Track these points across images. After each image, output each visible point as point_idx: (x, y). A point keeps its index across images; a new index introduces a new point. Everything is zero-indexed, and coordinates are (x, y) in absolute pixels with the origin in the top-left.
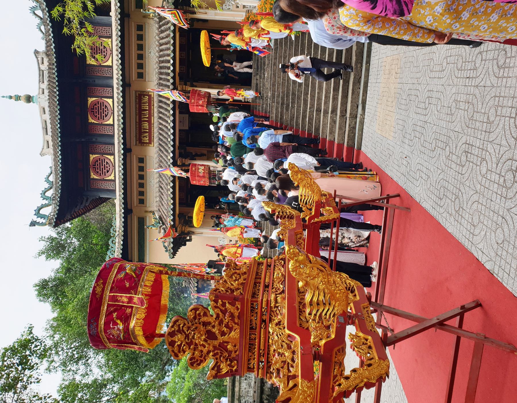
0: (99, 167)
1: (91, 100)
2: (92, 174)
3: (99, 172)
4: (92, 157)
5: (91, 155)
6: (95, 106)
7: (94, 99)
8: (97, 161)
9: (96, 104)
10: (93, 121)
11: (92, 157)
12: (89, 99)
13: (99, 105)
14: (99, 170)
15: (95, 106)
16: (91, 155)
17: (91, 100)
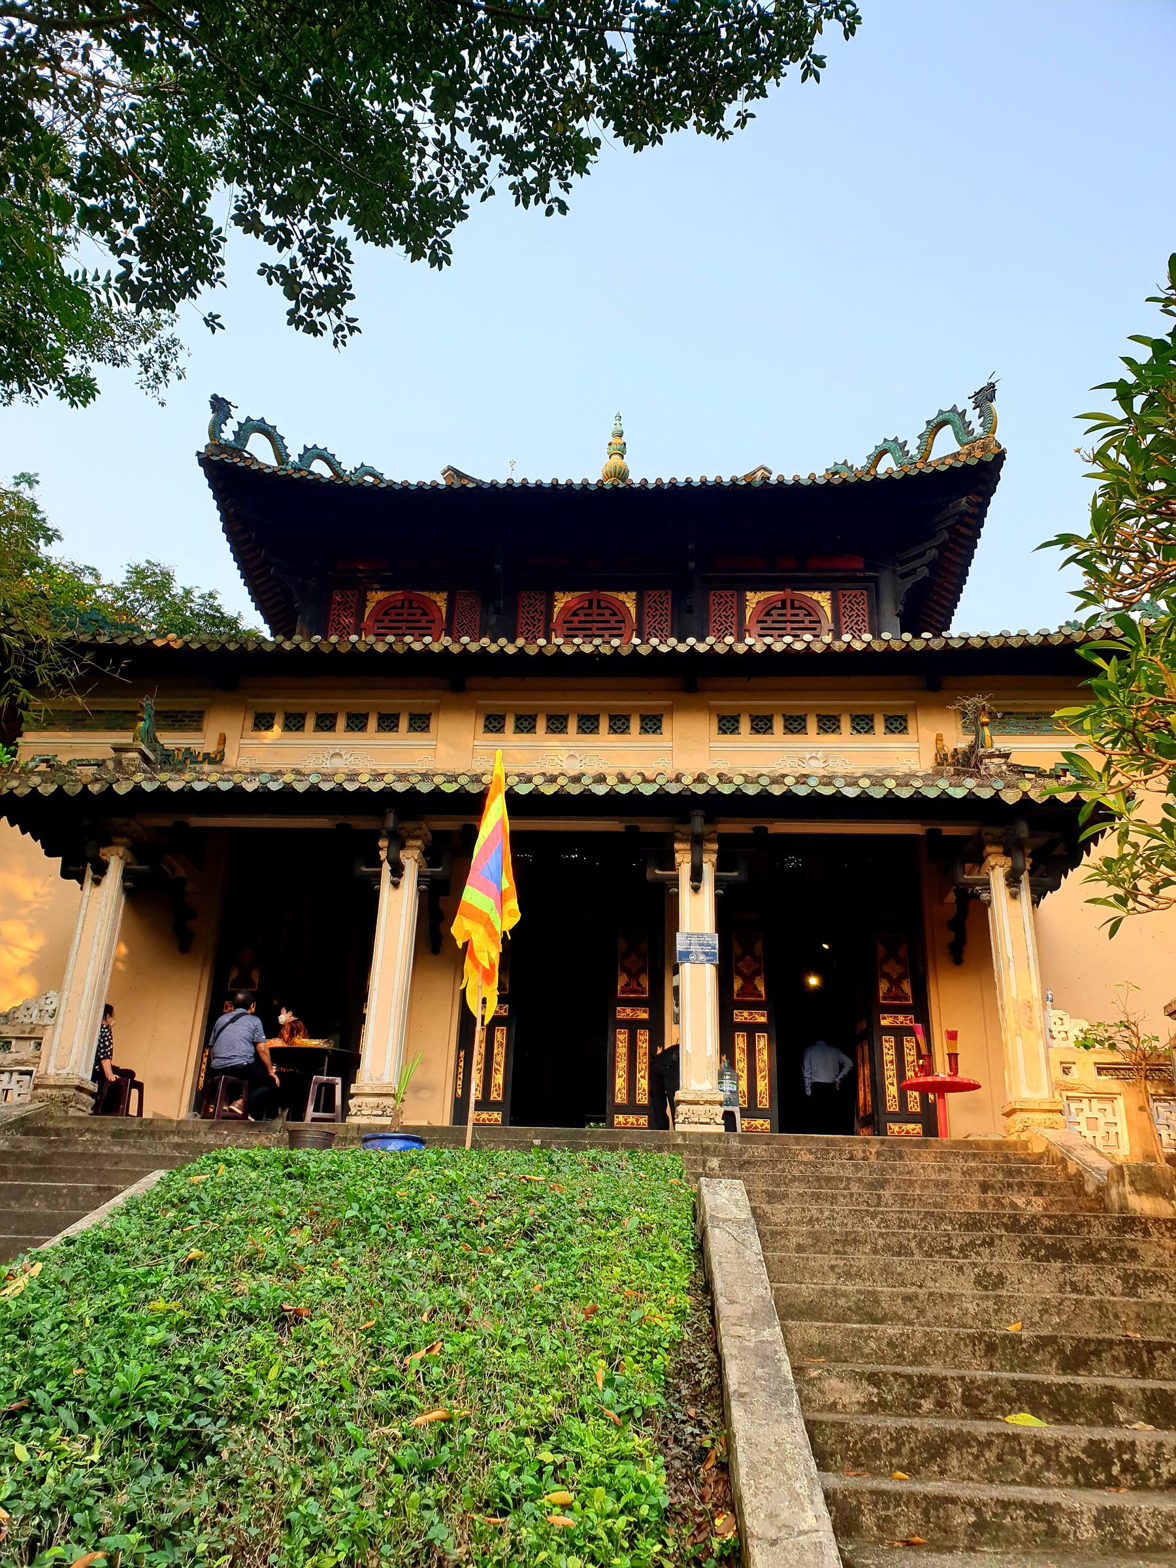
0: (405, 617)
1: (629, 600)
2: (381, 595)
3: (387, 619)
4: (440, 600)
5: (445, 595)
6: (607, 612)
7: (633, 611)
8: (425, 614)
9: (614, 614)
10: (558, 606)
11: (440, 600)
12: (633, 595)
13: (613, 624)
14: (394, 618)
15: (607, 612)
16: (445, 595)
17: (629, 600)
